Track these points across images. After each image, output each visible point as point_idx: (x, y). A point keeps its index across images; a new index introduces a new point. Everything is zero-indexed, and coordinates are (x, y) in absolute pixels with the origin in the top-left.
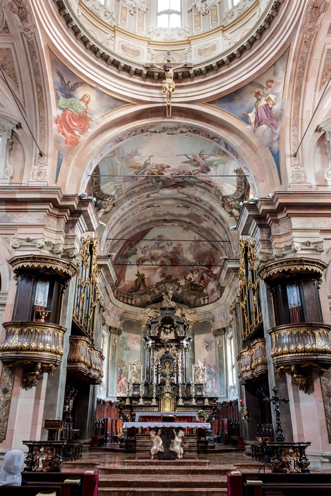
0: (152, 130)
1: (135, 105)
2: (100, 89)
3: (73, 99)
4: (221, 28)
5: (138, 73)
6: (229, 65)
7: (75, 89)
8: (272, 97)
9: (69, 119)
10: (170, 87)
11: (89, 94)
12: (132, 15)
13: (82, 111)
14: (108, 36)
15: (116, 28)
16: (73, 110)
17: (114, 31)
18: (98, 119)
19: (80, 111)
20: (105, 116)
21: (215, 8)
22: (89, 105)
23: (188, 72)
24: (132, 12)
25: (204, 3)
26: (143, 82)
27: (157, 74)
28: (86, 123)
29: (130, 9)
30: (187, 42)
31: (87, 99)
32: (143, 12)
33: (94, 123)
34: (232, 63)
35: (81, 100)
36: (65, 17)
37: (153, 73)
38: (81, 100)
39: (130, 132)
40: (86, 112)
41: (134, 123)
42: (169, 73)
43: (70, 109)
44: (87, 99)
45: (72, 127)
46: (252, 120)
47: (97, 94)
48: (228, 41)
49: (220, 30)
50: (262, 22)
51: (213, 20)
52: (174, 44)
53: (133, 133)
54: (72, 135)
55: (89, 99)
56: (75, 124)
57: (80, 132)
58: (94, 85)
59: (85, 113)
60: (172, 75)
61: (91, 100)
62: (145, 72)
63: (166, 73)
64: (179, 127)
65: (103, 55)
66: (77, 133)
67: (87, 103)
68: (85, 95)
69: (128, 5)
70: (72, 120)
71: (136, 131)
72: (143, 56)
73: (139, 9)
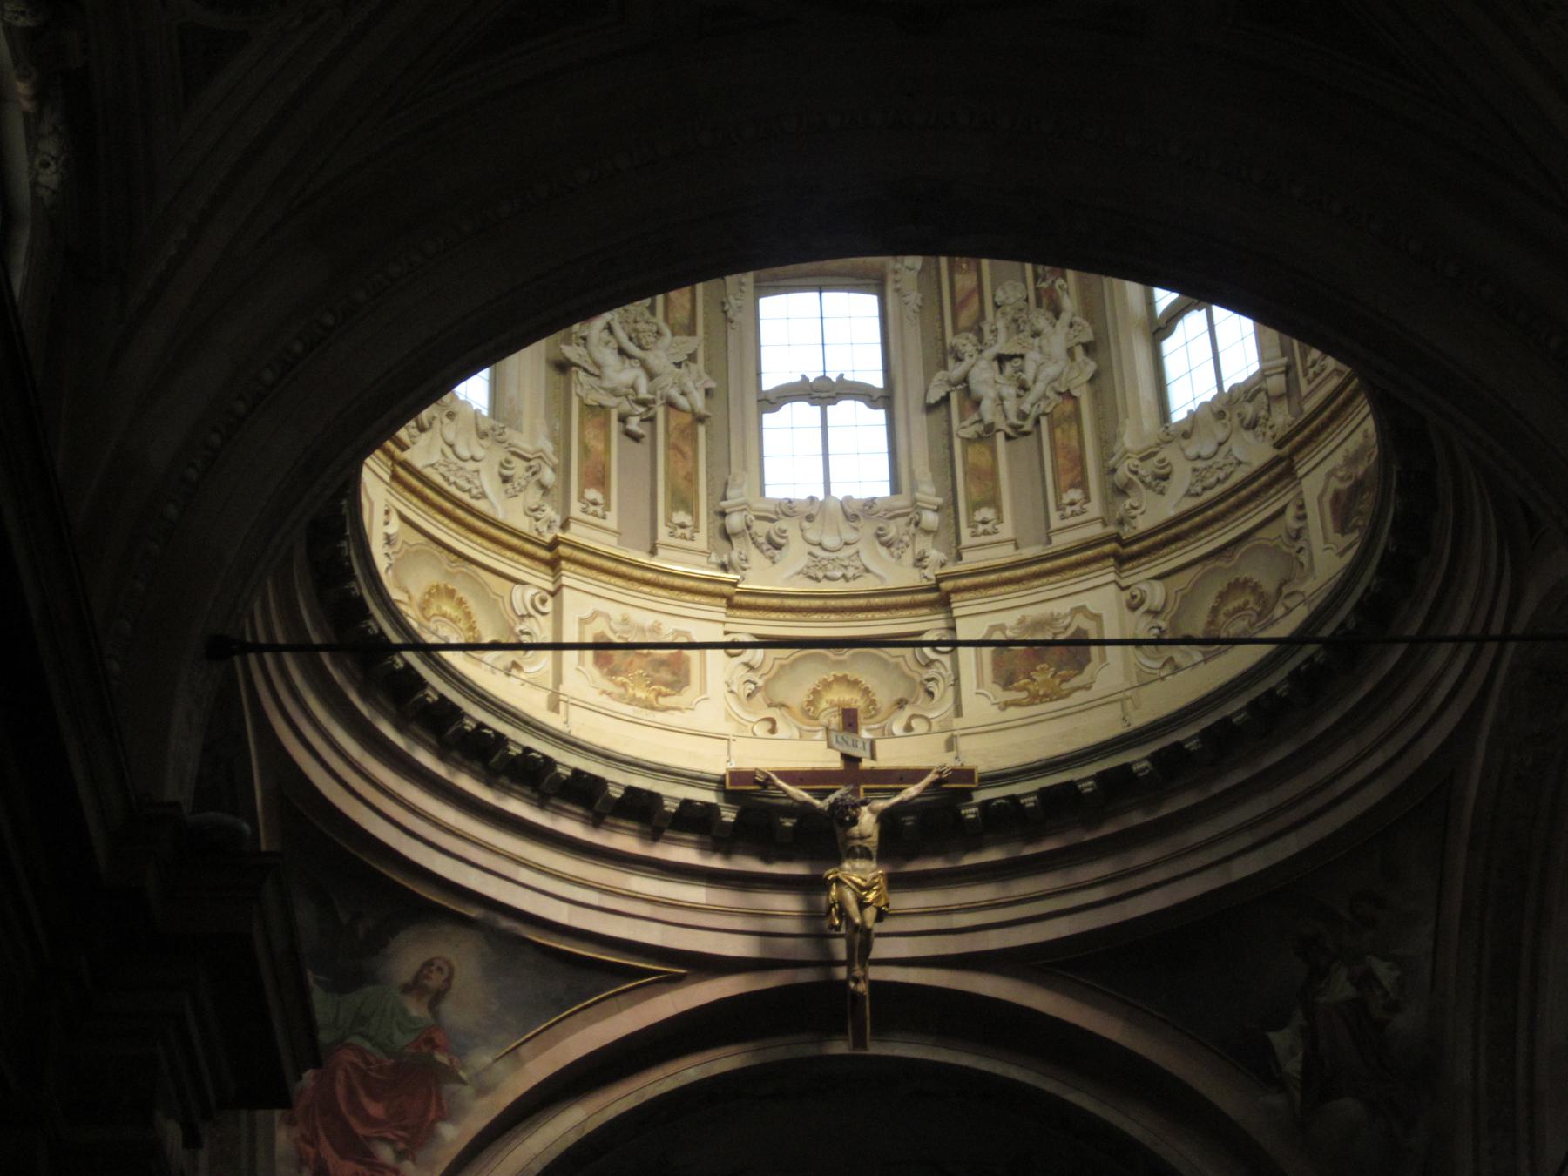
1: (673, 981)
2: (505, 923)
3: (369, 989)
4: (1107, 548)
8: (1382, 970)
9: (351, 1092)
10: (862, 905)
12: (636, 438)
14: (521, 597)
15: (563, 550)
16: (367, 1046)
17: (553, 565)
18: (488, 1069)
19: (402, 1040)
20: (524, 1050)
21: (1068, 407)
22: (447, 1008)
24: (634, 424)
25: (1009, 368)
26: (716, 862)
27: (788, 823)
29: (626, 407)
30: (933, 596)
31: (435, 981)
32: (687, 419)
33: (468, 1091)
35: (407, 989)
38: (407, 989)
40: (430, 1041)
41: (671, 1068)
42: (855, 830)
43: (356, 1040)
44: (435, 981)
45: (361, 1131)
46: (1292, 1066)
48: (1149, 618)
49: (1104, 557)
51: (1063, 483)
52: (862, 602)
54: (360, 1168)
55: (449, 980)
56: (375, 1109)
57: (401, 1146)
58: (474, 912)
59: (425, 1049)
61: (455, 982)
62: (729, 816)
63: (839, 830)
66: (386, 1154)
67: (437, 997)
68: (429, 964)
69: (614, 392)
70: (361, 1092)
72: (703, 688)
73: (671, 404)
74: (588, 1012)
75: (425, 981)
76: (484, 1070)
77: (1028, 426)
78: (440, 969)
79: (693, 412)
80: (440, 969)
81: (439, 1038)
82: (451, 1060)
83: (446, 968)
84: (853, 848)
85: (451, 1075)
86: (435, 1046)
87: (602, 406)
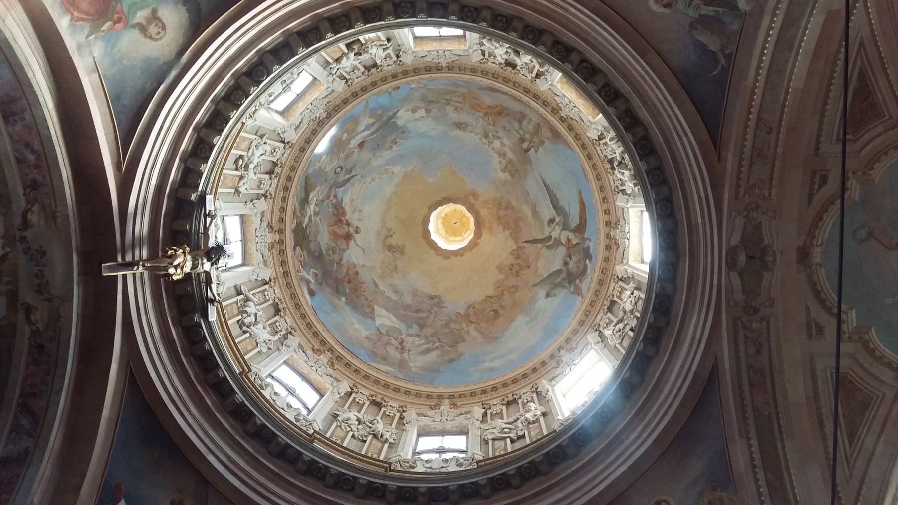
0: (33, 218)
1: (118, 166)
2: (173, 73)
5: (190, 176)
6: (224, 410)
7: (184, 4)
11: (159, 42)
13: (125, 9)
18: (91, 53)
22: (135, 34)
23: (193, 311)
28: (87, 14)
29: (246, 158)
31: (153, 29)
33: (82, 38)
34: (229, 417)
36: (343, 19)
37: (189, 217)
38: (154, 12)
39: (37, 146)
40: (119, 21)
42: (205, 260)
44: (153, 29)
47: (161, 62)
50: (336, 468)
53: (32, 157)
55: (151, 38)
59: (116, 16)
60: (199, 269)
61: (149, 40)
64: (49, 300)
65: (241, 93)
67: (143, 29)
68: (164, 28)
71: (37, 167)
73: (241, 178)
74: (109, 117)
75: (154, 24)
76: (91, 51)
77: (245, 328)
78: (159, 33)
79: (238, 187)
80: (159, 33)
81: (119, 26)
82: (104, 31)
83: (158, 37)
84: (198, 260)
85: (95, 30)
86: (115, 23)
87: (249, 149)
